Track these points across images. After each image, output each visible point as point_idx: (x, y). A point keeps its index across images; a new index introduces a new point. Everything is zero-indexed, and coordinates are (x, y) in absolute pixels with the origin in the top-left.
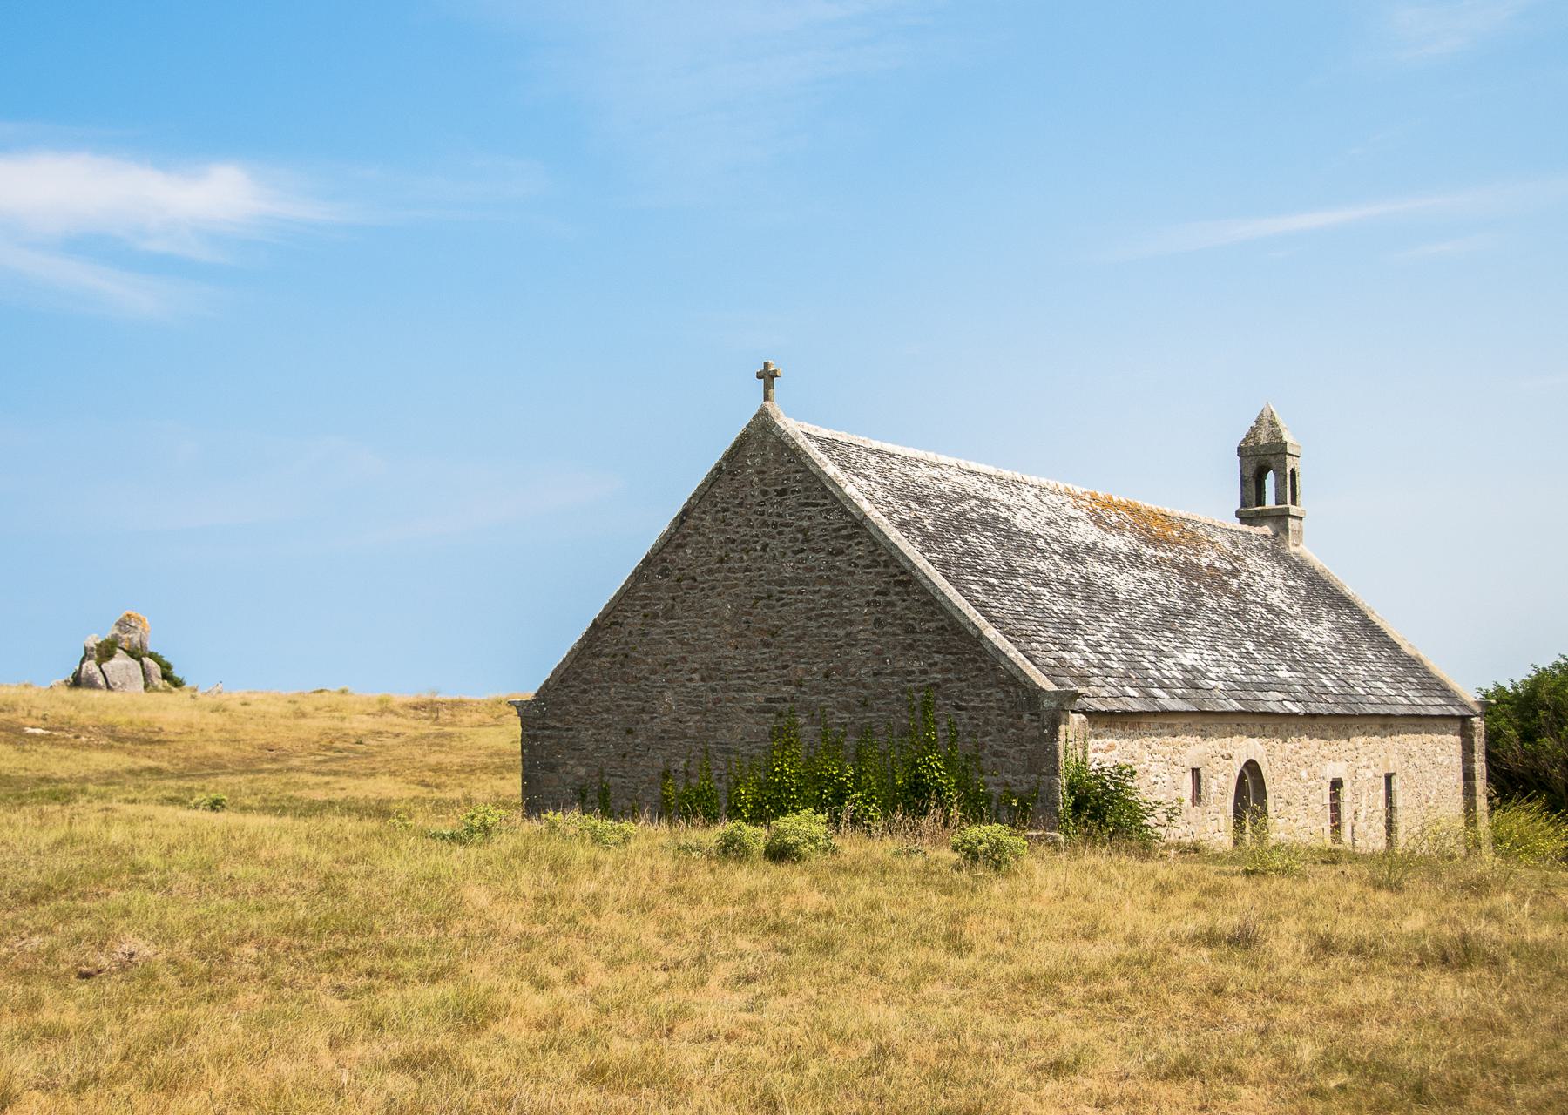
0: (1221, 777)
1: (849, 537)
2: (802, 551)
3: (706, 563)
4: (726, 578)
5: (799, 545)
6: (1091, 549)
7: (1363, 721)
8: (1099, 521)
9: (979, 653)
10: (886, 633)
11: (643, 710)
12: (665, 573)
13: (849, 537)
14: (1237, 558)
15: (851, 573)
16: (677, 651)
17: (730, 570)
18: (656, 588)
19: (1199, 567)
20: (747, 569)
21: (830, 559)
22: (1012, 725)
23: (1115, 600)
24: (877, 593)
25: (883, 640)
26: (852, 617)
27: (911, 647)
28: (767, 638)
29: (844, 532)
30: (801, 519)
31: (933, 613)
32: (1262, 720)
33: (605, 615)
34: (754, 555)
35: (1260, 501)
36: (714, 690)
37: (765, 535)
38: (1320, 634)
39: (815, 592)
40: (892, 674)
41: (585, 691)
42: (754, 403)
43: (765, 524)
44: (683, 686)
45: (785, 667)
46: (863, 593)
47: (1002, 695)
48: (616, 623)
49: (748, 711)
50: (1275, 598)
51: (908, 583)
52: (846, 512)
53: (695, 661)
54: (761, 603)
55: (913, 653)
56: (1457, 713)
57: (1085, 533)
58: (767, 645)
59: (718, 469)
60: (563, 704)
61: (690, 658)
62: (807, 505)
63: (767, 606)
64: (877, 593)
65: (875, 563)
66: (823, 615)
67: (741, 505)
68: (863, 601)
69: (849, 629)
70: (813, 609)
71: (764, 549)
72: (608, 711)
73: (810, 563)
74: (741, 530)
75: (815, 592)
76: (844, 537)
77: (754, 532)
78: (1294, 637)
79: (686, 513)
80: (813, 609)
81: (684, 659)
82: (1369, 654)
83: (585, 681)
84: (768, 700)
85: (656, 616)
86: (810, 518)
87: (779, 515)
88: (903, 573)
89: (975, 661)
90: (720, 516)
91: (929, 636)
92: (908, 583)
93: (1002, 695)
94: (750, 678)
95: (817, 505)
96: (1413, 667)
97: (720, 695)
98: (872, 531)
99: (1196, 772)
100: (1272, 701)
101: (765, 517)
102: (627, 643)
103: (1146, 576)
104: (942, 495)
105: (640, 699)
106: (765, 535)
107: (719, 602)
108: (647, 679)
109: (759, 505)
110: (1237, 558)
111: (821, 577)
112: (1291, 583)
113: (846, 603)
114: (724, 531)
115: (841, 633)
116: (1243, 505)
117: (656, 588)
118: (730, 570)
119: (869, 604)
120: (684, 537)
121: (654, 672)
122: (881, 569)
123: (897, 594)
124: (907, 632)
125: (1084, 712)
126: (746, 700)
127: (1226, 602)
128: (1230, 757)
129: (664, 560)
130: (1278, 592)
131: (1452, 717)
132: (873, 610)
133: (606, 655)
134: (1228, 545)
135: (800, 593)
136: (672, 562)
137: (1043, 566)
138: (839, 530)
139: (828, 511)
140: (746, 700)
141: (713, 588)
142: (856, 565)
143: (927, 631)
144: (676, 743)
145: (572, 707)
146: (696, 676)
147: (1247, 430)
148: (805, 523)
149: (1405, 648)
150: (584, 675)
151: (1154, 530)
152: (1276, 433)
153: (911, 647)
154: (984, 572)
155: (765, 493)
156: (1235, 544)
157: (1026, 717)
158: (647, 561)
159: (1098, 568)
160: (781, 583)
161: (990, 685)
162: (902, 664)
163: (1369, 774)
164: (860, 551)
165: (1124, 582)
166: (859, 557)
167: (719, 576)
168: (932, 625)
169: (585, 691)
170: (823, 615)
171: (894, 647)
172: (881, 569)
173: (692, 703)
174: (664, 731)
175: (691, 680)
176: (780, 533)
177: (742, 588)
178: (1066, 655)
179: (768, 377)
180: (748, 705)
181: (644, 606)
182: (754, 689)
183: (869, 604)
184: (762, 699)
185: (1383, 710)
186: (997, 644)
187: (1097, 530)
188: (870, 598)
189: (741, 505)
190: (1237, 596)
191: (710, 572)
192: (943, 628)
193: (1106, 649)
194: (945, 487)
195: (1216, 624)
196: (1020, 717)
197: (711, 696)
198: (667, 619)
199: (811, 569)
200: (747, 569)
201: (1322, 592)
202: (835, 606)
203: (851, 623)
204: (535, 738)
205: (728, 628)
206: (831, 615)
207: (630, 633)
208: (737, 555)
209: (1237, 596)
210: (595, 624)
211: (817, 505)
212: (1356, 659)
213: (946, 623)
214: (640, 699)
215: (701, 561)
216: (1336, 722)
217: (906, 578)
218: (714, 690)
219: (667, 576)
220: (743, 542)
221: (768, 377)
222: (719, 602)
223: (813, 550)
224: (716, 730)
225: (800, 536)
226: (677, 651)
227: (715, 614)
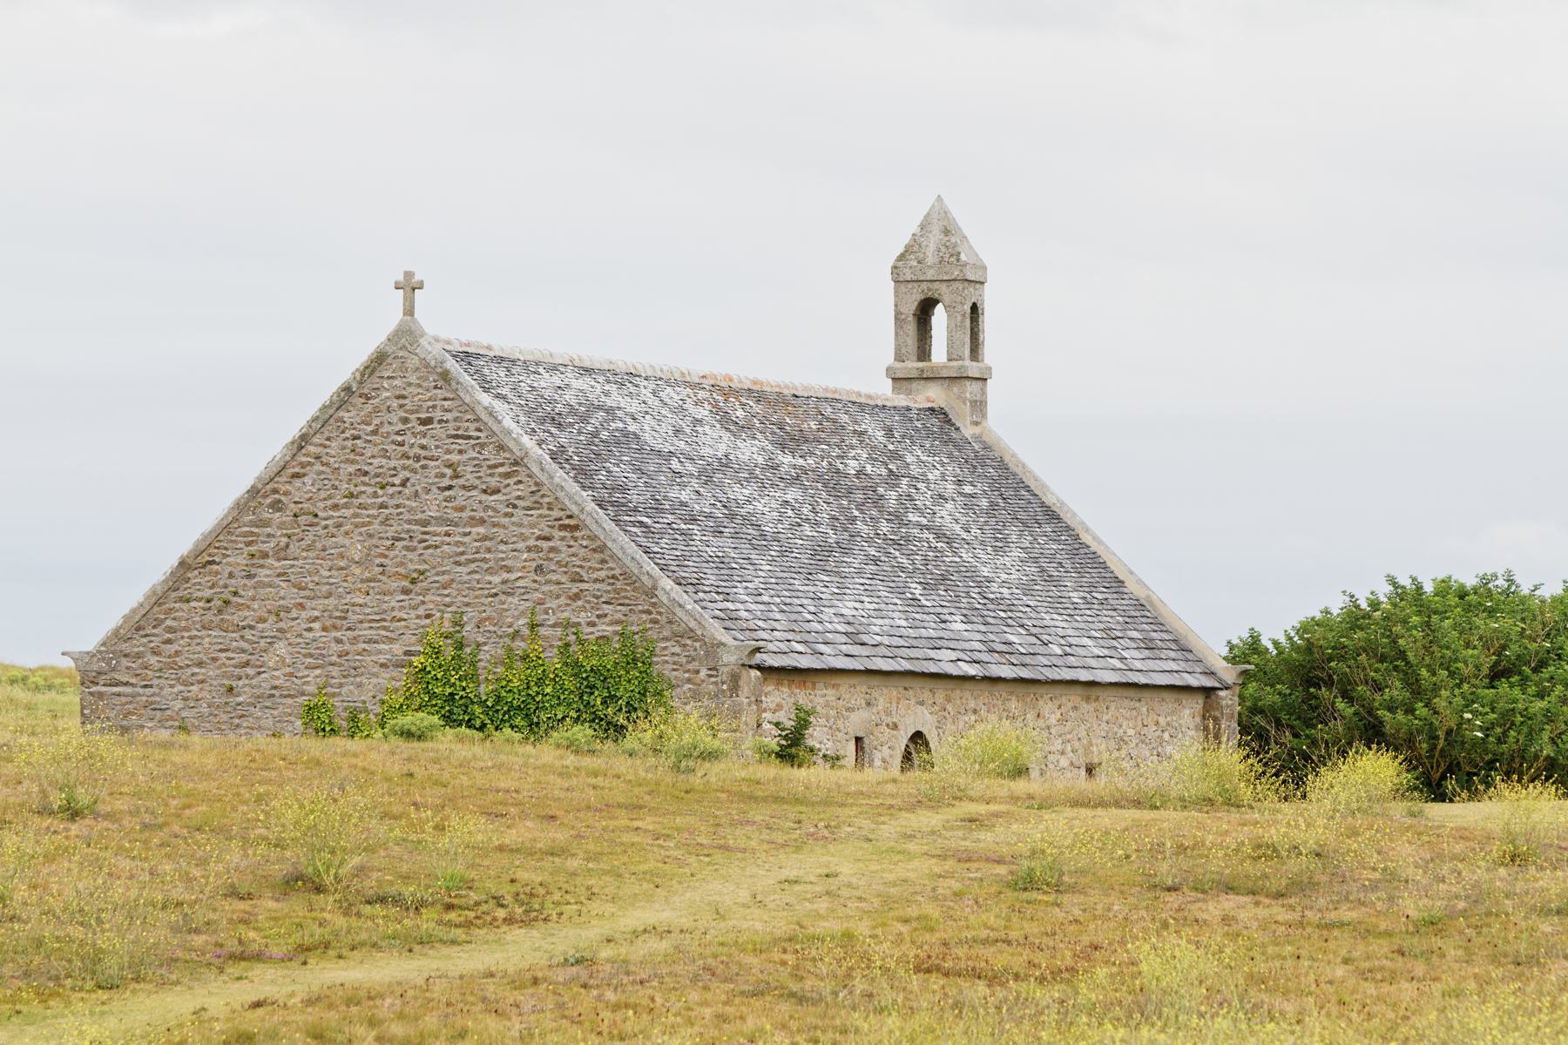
0: (886, 751)
1: (507, 475)
2: (450, 488)
3: (330, 497)
4: (356, 515)
5: (446, 482)
6: (725, 463)
7: (1057, 690)
8: (726, 421)
9: (654, 604)
10: (548, 582)
11: (247, 664)
12: (277, 506)
13: (507, 475)
14: (895, 456)
15: (506, 515)
16: (290, 596)
17: (360, 506)
18: (266, 523)
19: (846, 476)
20: (383, 506)
21: (484, 497)
22: (689, 681)
23: (763, 536)
24: (539, 538)
25: (546, 588)
26: (509, 563)
27: (576, 597)
28: (406, 583)
29: (501, 470)
30: (449, 452)
31: (603, 561)
32: (930, 684)
33: (198, 552)
34: (391, 490)
35: (924, 353)
36: (339, 641)
37: (404, 468)
38: (1005, 570)
39: (466, 534)
40: (554, 626)
41: (169, 642)
42: (395, 317)
43: (405, 456)
44: (300, 636)
45: (428, 616)
46: (524, 538)
47: (677, 650)
48: (213, 562)
49: (382, 665)
50: (948, 516)
51: (576, 528)
52: (501, 447)
53: (315, 608)
54: (399, 544)
55: (580, 603)
56: (1194, 681)
57: (715, 442)
58: (406, 592)
59: (347, 389)
60: (139, 655)
61: (308, 604)
62: (457, 436)
63: (407, 548)
64: (539, 538)
65: (538, 505)
66: (473, 561)
67: (375, 432)
68: (521, 545)
69: (505, 576)
70: (463, 553)
71: (403, 484)
72: (200, 664)
73: (460, 502)
74: (375, 461)
75: (466, 534)
76: (500, 475)
77: (393, 463)
78: (971, 574)
79: (303, 440)
80: (463, 553)
81: (302, 606)
82: (1076, 597)
83: (170, 630)
84: (408, 653)
85: (265, 555)
86: (460, 452)
87: (423, 447)
88: (570, 517)
89: (650, 613)
90: (349, 443)
91: (597, 586)
92: (576, 528)
93: (677, 650)
94: (385, 628)
95: (470, 437)
96: (1143, 611)
97: (347, 647)
98: (535, 469)
99: (858, 740)
100: (945, 662)
101: (406, 448)
102: (226, 586)
103: (789, 497)
104: (573, 411)
105: (244, 651)
106: (404, 468)
107: (347, 542)
108: (251, 627)
109: (397, 433)
110: (895, 456)
111: (472, 518)
112: (968, 489)
113: (503, 547)
114: (353, 462)
115: (496, 579)
116: (899, 357)
117: (266, 523)
118: (360, 506)
119: (529, 549)
120: (303, 465)
121: (262, 620)
122: (544, 512)
123: (563, 539)
124: (573, 581)
125: (758, 667)
126: (380, 652)
127: (884, 527)
128: (895, 727)
129: (275, 491)
130: (949, 506)
131: (1187, 689)
132: (533, 555)
133: (199, 600)
134: (880, 434)
135: (448, 534)
136: (286, 493)
137: (684, 496)
138: (495, 466)
139: (482, 446)
140: (380, 652)
141: (339, 526)
142: (515, 507)
143: (596, 581)
144: (289, 701)
145: (153, 660)
146: (316, 625)
147: (907, 239)
148: (455, 458)
149: (1131, 586)
150: (169, 623)
151: (793, 420)
152: (950, 254)
153: (576, 597)
154: (635, 510)
155: (405, 421)
156: (889, 432)
157: (704, 673)
158: (254, 492)
159: (739, 493)
160: (425, 523)
161: (666, 639)
162: (566, 615)
163: (1064, 762)
164: (522, 490)
165: (765, 507)
166: (519, 498)
167: (347, 513)
168: (603, 574)
169: (169, 642)
170: (473, 561)
171: (558, 597)
172: (544, 512)
173: (311, 656)
174: (275, 688)
175: (310, 630)
176: (424, 467)
177: (376, 527)
178: (730, 605)
179: (410, 287)
180: (382, 659)
181: (249, 544)
182: (391, 640)
183: (529, 549)
184: (400, 652)
185: (1084, 676)
186: (673, 595)
187: (726, 436)
188: (532, 542)
189: (375, 432)
190: (897, 518)
191: (336, 507)
192: (613, 577)
193: (765, 598)
194: (569, 397)
195: (876, 561)
196: (698, 672)
197: (335, 647)
198: (279, 560)
199: (462, 509)
200: (383, 506)
201: (1013, 499)
202: (489, 550)
203: (509, 570)
204: (101, 695)
205: (357, 571)
206: (484, 560)
207: (231, 575)
208: (370, 490)
209: (897, 518)
210: (183, 564)
211: (470, 437)
212: (1056, 605)
213: (617, 572)
214: (244, 651)
215: (323, 494)
216: (1021, 689)
217: (571, 522)
218: (339, 641)
219: (280, 510)
220: (377, 475)
221: (410, 287)
222: (347, 542)
223: (464, 487)
224: (341, 685)
225: (449, 472)
226: (290, 596)
227: (342, 556)
